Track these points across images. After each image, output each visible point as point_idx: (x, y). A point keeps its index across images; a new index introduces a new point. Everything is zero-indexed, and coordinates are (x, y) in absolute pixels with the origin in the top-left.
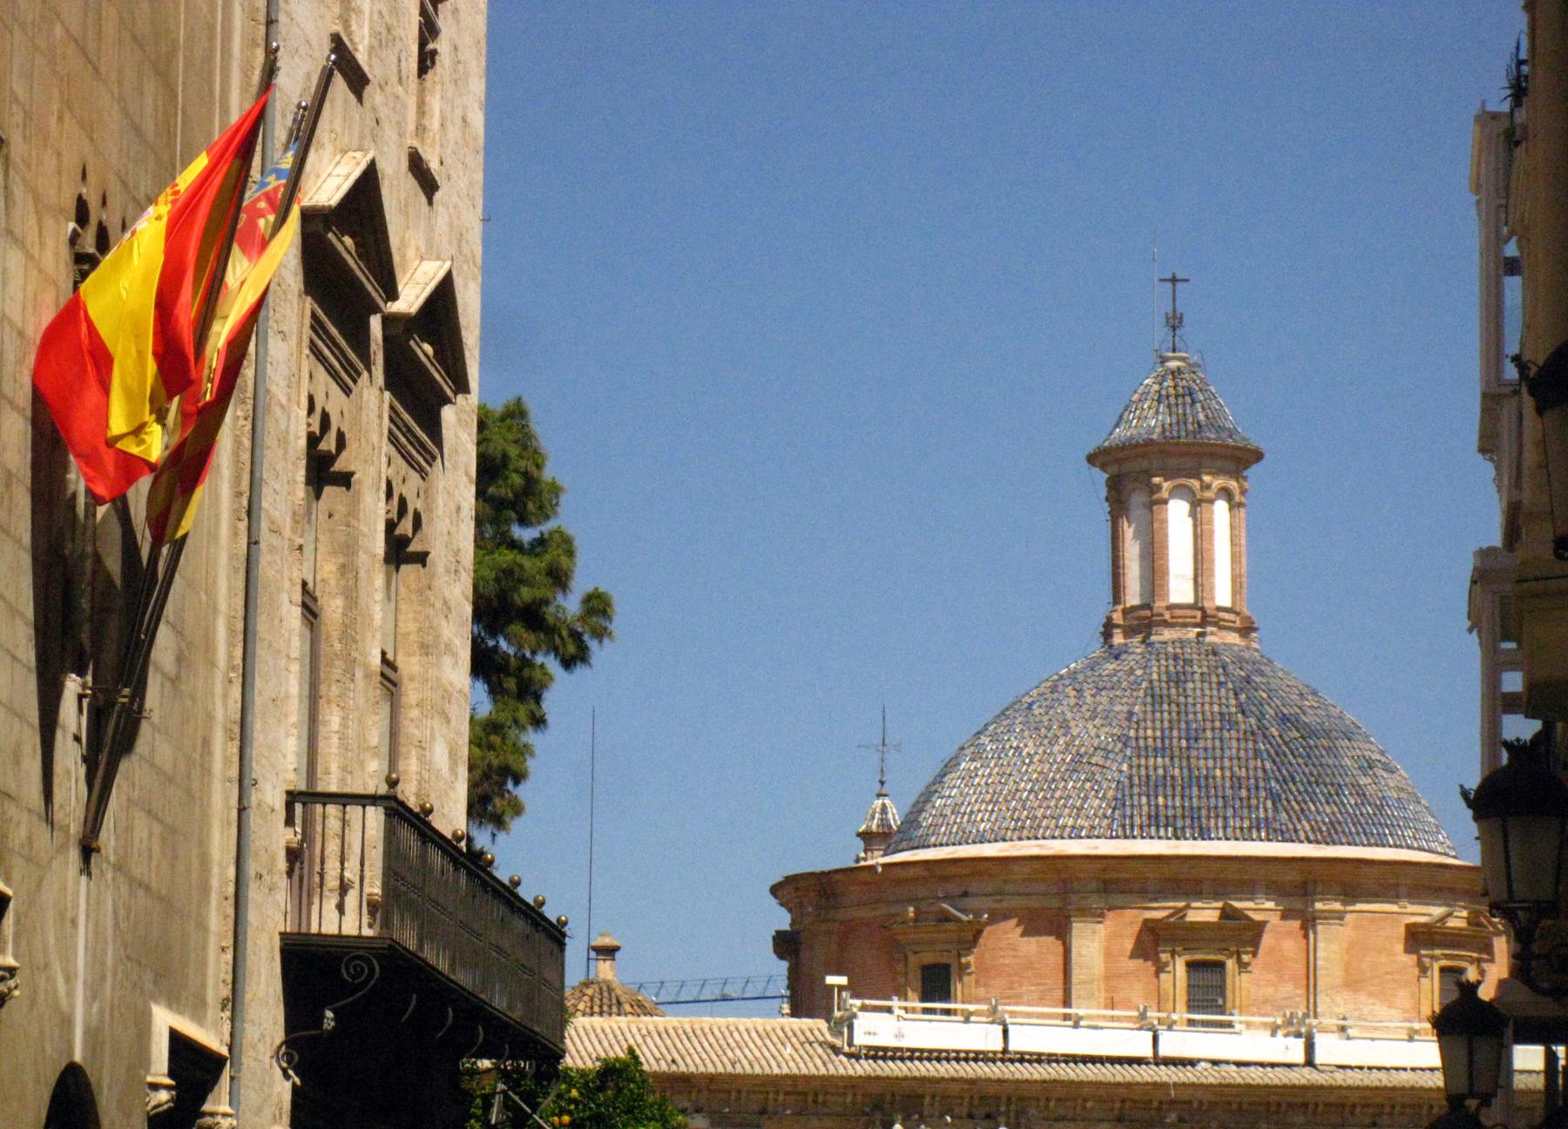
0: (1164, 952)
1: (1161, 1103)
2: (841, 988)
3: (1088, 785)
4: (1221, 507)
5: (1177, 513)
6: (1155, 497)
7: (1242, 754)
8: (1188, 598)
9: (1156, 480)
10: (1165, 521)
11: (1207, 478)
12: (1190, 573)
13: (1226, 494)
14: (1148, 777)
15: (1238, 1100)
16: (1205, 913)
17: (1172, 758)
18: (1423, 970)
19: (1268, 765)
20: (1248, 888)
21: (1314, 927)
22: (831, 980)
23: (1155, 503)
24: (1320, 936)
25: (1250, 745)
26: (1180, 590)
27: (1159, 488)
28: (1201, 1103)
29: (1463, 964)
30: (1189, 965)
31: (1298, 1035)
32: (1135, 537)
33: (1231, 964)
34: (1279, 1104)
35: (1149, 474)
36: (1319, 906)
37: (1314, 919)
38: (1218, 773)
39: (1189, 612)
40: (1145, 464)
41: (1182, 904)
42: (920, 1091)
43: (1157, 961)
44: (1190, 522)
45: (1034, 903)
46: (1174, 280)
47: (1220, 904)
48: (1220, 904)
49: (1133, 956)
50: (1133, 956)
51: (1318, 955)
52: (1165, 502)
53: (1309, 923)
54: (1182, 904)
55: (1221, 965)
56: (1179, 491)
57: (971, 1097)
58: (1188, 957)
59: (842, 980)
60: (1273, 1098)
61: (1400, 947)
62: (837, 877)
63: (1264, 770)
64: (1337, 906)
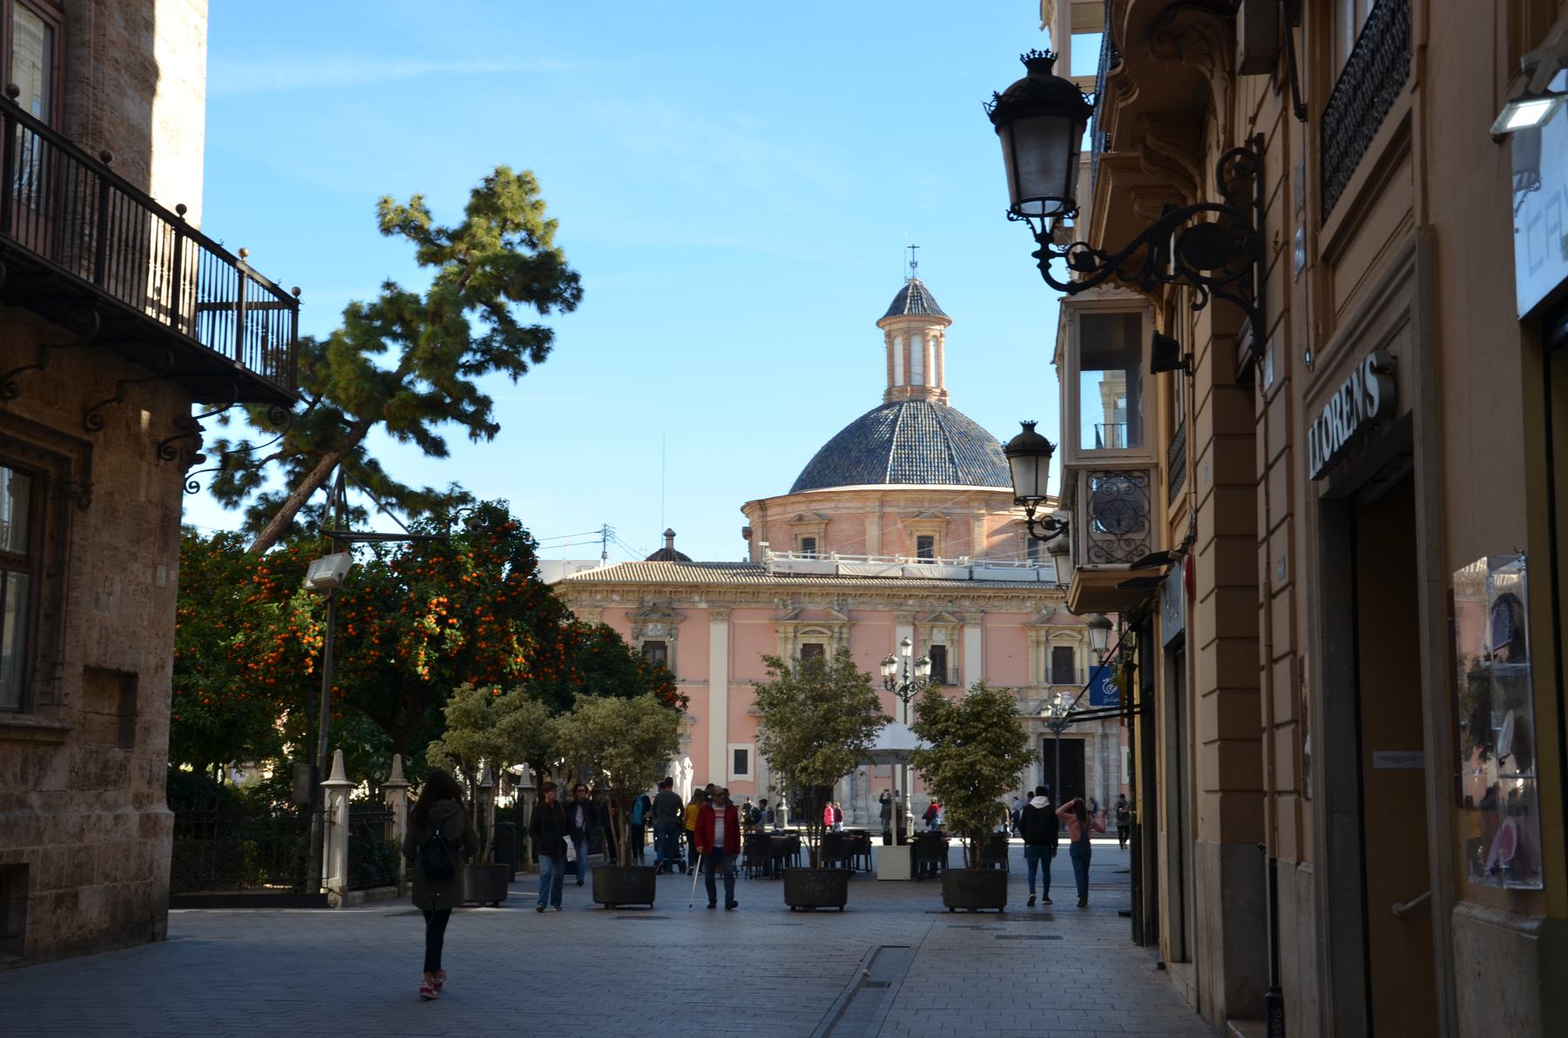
46: (913, 247)
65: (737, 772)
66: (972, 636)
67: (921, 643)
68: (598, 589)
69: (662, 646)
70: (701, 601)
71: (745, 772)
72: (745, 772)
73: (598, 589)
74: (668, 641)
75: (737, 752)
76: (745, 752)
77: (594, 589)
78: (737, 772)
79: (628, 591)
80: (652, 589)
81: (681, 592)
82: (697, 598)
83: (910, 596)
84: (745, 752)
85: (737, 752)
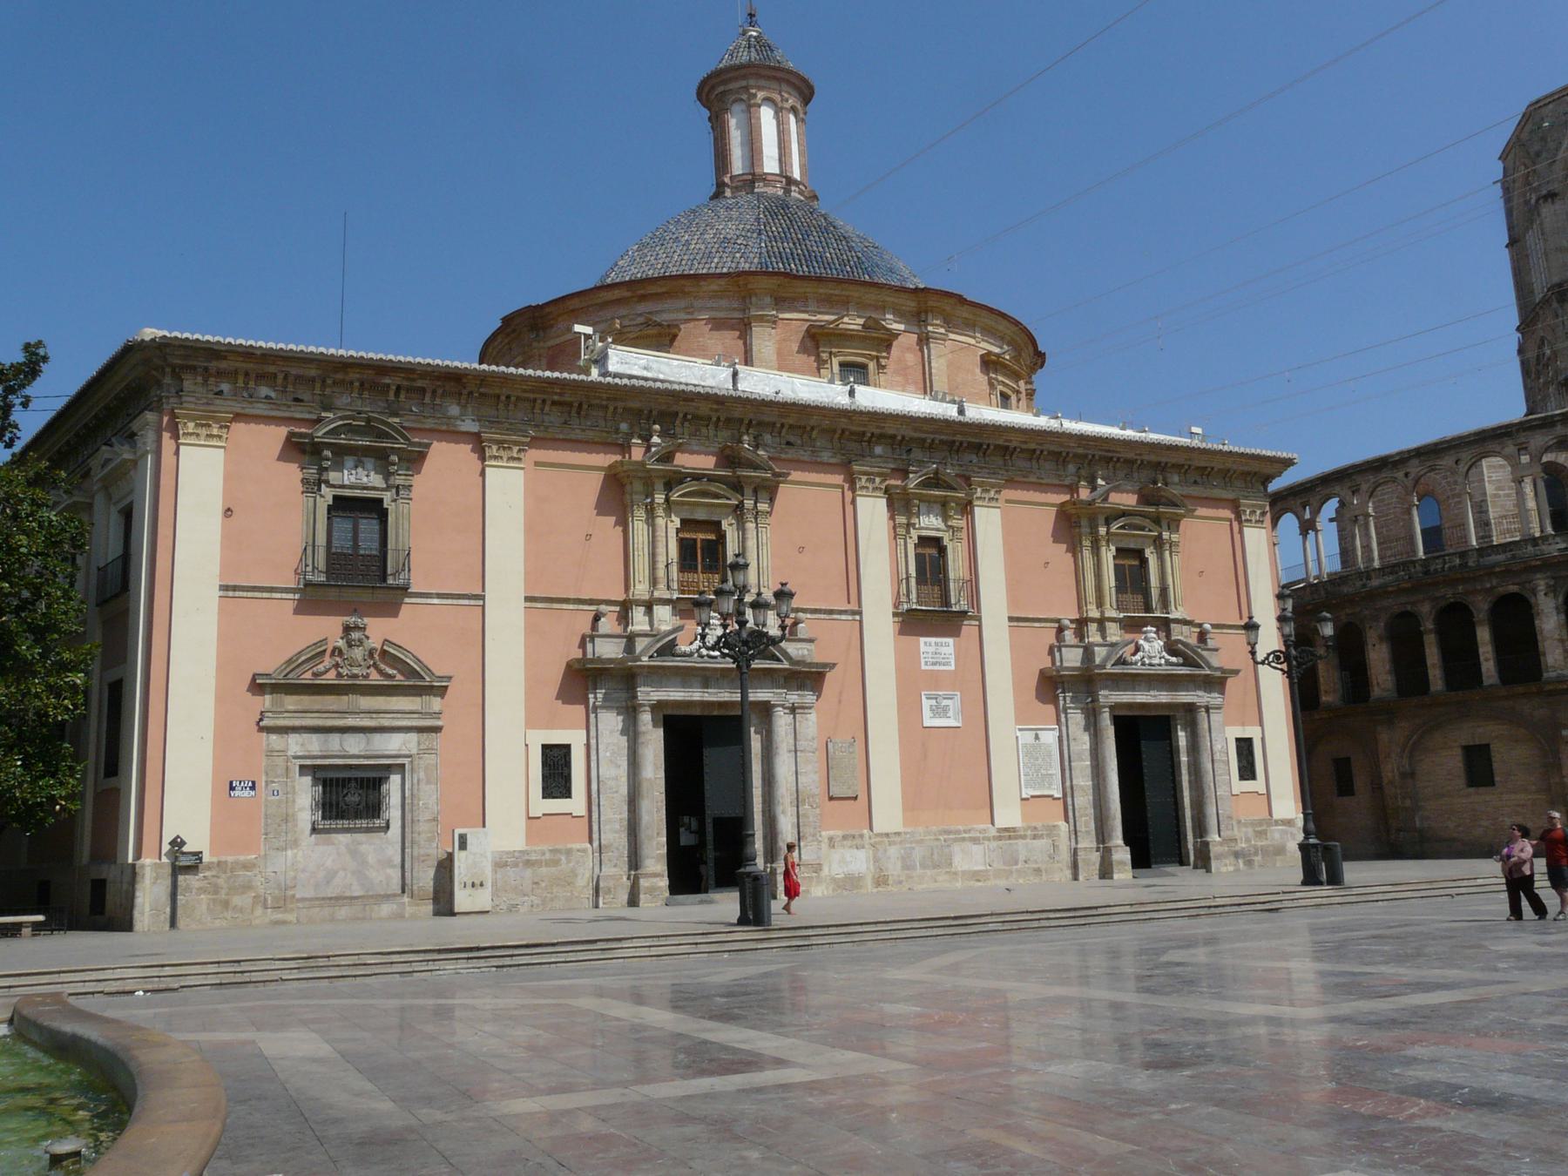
0: (824, 352)
1: (873, 434)
2: (588, 337)
3: (738, 255)
4: (792, 118)
5: (767, 115)
6: (752, 102)
7: (841, 247)
8: (777, 171)
9: (754, 91)
10: (759, 118)
11: (786, 95)
12: (777, 156)
13: (793, 109)
14: (780, 253)
15: (932, 436)
16: (853, 323)
17: (794, 244)
18: (991, 385)
19: (860, 255)
20: (883, 308)
21: (928, 344)
22: (578, 328)
23: (751, 109)
24: (933, 352)
25: (844, 243)
26: (770, 165)
27: (755, 96)
28: (903, 437)
29: (1010, 393)
30: (842, 365)
31: (953, 402)
32: (738, 127)
33: (872, 366)
34: (961, 443)
35: (746, 88)
36: (930, 328)
37: (928, 339)
38: (828, 255)
39: (778, 178)
40: (744, 83)
41: (833, 318)
42: (674, 408)
43: (818, 356)
44: (774, 122)
45: (721, 315)
47: (861, 321)
48: (861, 321)
49: (798, 352)
50: (798, 352)
51: (932, 365)
52: (759, 106)
53: (924, 340)
54: (833, 318)
55: (864, 367)
56: (767, 100)
57: (718, 418)
58: (842, 358)
59: (589, 330)
60: (959, 438)
61: (978, 370)
62: (547, 310)
63: (858, 258)
64: (942, 330)
65: (548, 793)
66: (989, 520)
67: (901, 531)
68: (223, 365)
69: (375, 508)
70: (461, 417)
71: (566, 793)
72: (566, 793)
73: (223, 365)
74: (387, 497)
75: (546, 748)
76: (566, 748)
77: (214, 365)
78: (548, 793)
79: (298, 378)
80: (353, 375)
81: (423, 391)
82: (454, 410)
83: (882, 436)
84: (566, 748)
85: (546, 748)
